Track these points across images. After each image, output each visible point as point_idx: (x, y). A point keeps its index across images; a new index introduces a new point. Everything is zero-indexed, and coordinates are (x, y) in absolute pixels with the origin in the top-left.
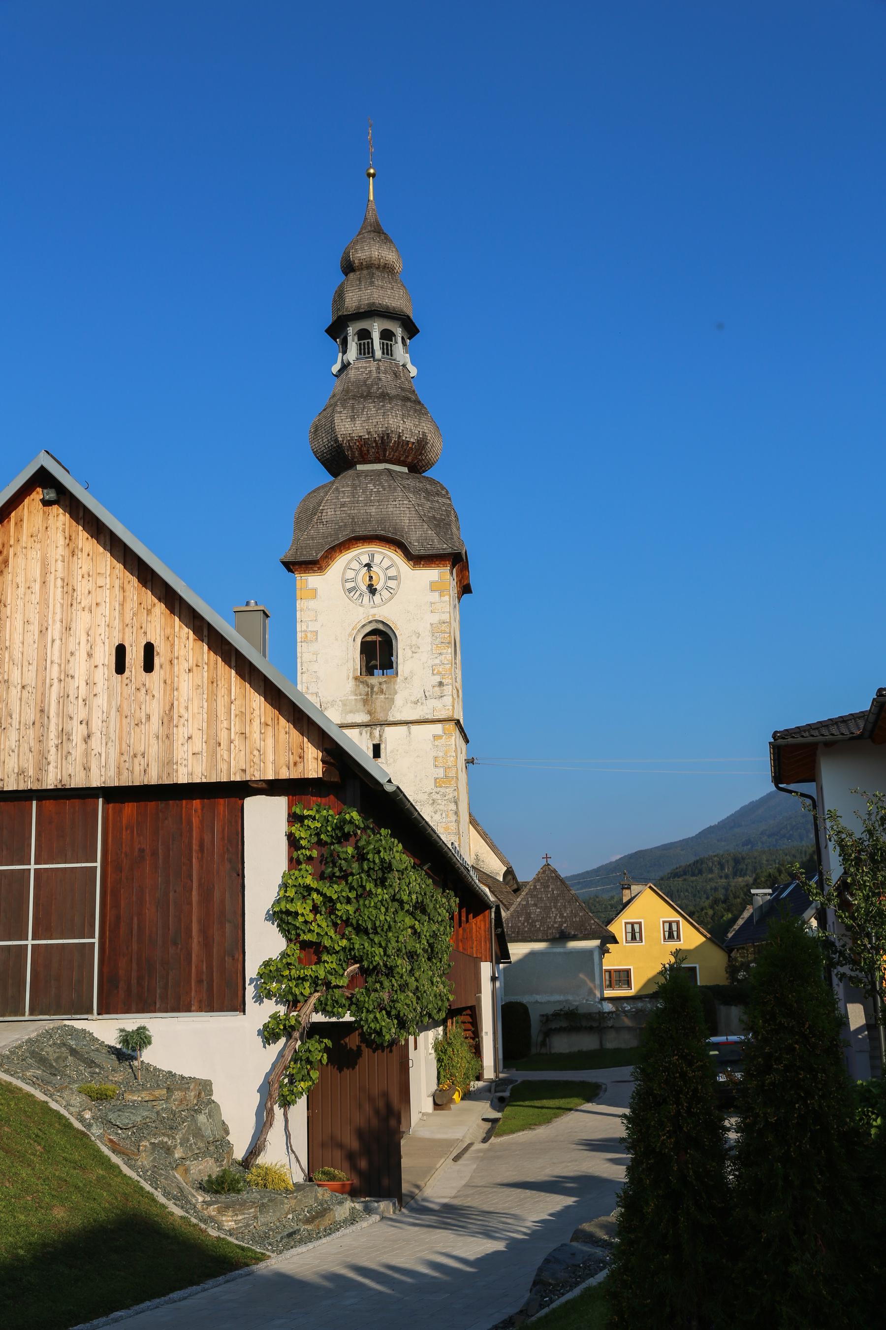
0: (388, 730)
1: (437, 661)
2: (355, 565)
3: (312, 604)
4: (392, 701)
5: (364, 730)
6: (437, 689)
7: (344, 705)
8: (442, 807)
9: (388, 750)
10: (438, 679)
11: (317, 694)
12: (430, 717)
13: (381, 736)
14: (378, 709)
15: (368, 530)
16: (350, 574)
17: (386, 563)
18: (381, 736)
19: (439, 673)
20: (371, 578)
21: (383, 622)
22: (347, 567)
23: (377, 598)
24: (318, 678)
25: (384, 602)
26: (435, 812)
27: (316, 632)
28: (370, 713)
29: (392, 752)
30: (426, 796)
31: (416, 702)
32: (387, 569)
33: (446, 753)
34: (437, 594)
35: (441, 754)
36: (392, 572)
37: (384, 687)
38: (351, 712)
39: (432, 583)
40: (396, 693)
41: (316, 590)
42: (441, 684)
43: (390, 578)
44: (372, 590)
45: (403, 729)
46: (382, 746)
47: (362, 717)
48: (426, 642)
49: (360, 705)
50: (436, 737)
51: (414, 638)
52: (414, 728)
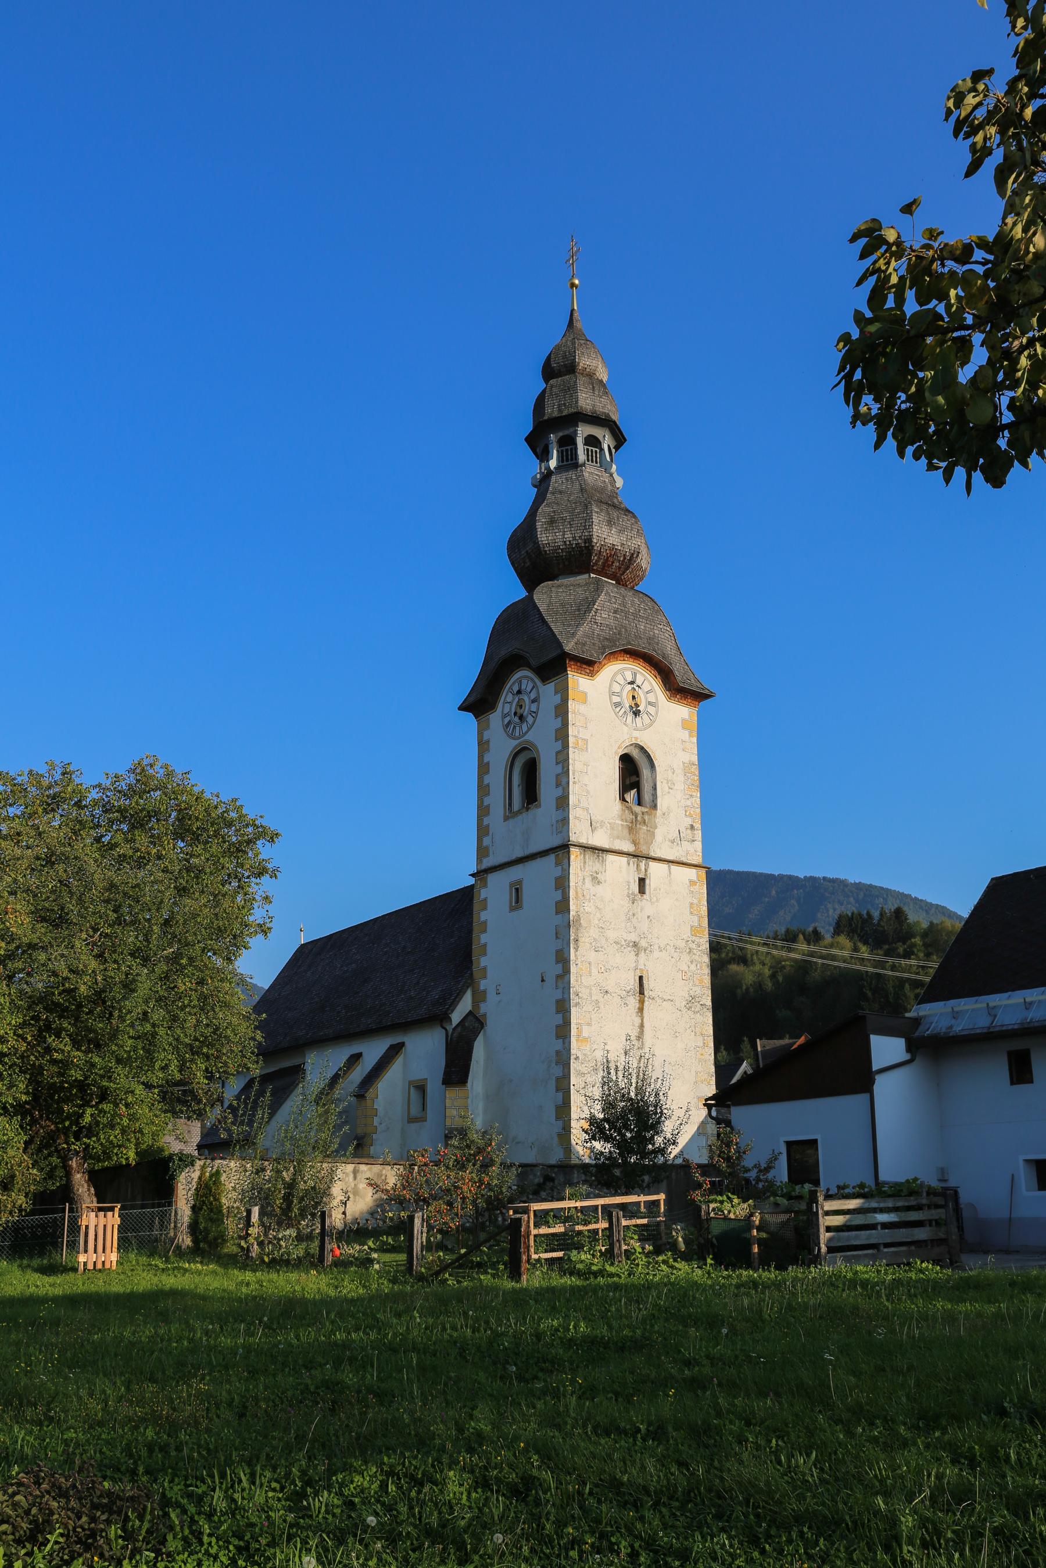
0: (653, 865)
1: (689, 803)
2: (619, 679)
3: (582, 708)
4: (653, 834)
5: (633, 860)
6: (689, 831)
7: (612, 828)
8: (696, 958)
9: (653, 886)
10: (689, 821)
11: (587, 809)
12: (684, 860)
13: (646, 870)
14: (642, 841)
15: (642, 646)
16: (616, 688)
17: (646, 687)
18: (646, 870)
19: (690, 816)
20: (634, 697)
21: (642, 748)
22: (613, 680)
23: (638, 719)
24: (588, 792)
25: (646, 728)
26: (692, 962)
27: (586, 741)
28: (635, 843)
29: (655, 890)
30: (682, 944)
31: (673, 842)
32: (647, 693)
33: (699, 901)
34: (687, 733)
35: (695, 901)
36: (651, 698)
37: (646, 817)
38: (618, 837)
39: (684, 721)
40: (656, 827)
41: (586, 694)
42: (692, 827)
43: (650, 703)
44: (637, 713)
45: (664, 867)
46: (647, 882)
47: (627, 847)
48: (679, 780)
49: (626, 832)
50: (692, 883)
51: (670, 772)
52: (674, 868)
